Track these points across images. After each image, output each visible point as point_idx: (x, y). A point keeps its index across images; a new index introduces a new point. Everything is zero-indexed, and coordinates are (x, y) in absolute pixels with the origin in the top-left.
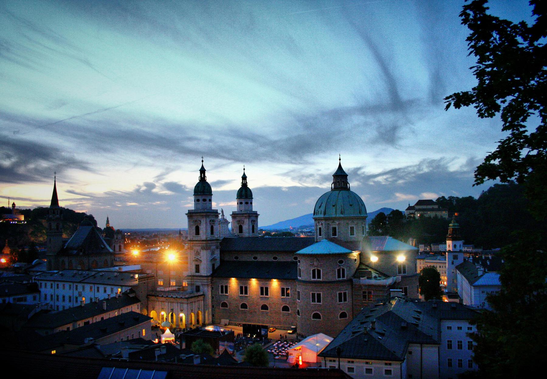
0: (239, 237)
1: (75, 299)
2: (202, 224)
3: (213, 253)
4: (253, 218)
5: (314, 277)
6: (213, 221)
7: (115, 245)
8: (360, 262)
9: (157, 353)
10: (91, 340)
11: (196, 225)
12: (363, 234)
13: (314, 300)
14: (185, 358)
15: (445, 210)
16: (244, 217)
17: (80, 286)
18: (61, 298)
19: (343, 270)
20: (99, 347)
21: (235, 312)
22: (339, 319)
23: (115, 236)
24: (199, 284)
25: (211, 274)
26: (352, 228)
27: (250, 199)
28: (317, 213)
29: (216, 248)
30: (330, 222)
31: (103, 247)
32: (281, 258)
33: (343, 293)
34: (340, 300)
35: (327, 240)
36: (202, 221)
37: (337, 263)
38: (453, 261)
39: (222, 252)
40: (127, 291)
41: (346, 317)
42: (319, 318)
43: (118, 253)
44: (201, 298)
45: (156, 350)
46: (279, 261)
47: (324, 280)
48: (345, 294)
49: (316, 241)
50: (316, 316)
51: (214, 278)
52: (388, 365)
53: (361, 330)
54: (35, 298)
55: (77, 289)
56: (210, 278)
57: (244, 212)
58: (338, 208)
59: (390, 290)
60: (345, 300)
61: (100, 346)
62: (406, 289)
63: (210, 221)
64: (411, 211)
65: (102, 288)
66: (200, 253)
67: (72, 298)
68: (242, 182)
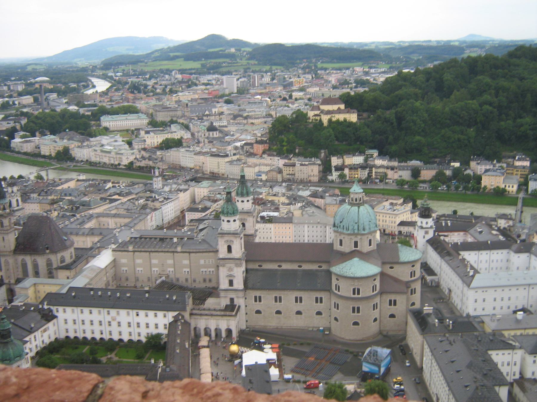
1: (107, 324)
5: (354, 294)
7: (11, 200)
13: (354, 311)
15: (354, 112)
17: (113, 312)
18: (87, 323)
19: (376, 285)
24: (232, 296)
26: (370, 241)
30: (353, 237)
31: (66, 239)
34: (374, 309)
36: (235, 242)
39: (247, 261)
48: (377, 303)
50: (356, 324)
54: (54, 325)
55: (109, 314)
58: (360, 225)
60: (377, 308)
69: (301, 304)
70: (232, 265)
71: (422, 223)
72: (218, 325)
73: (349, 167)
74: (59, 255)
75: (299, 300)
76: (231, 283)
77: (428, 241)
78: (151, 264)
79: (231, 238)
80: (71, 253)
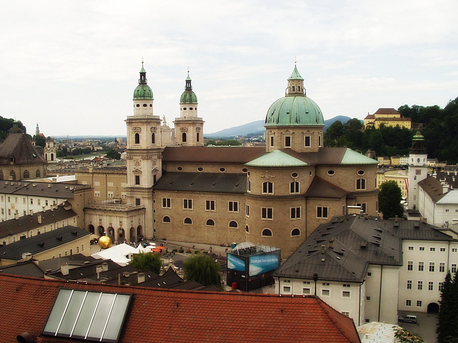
0: (182, 146)
2: (142, 131)
3: (154, 164)
4: (198, 126)
5: (265, 191)
6: (155, 128)
8: (315, 176)
9: (99, 270)
10: (29, 255)
11: (136, 133)
12: (320, 145)
13: (264, 216)
14: (128, 276)
15: (408, 120)
16: (188, 125)
17: (13, 198)
19: (297, 184)
20: (37, 262)
21: (178, 227)
22: (292, 236)
23: (47, 144)
24: (139, 196)
25: (152, 186)
26: (307, 139)
27: (194, 104)
28: (269, 120)
29: (158, 158)
31: (35, 156)
32: (230, 170)
33: (296, 209)
34: (293, 217)
35: (280, 151)
37: (291, 176)
38: (416, 176)
40: (62, 203)
41: (299, 234)
42: (271, 235)
43: (49, 162)
44: (142, 211)
45: (98, 267)
46: (226, 173)
47: (276, 195)
49: (267, 151)
51: (156, 191)
52: (347, 286)
53: (317, 249)
56: (151, 190)
57: (189, 119)
58: (292, 115)
59: (348, 206)
60: (298, 216)
61: (39, 262)
62: (364, 205)
63: (151, 129)
64: (371, 121)
65: (35, 200)
66: (140, 163)
67: (4, 210)
68: (186, 85)
69: (212, 211)
70: (139, 158)
71: (413, 159)
72: (111, 224)
73: (395, 166)
74: (23, 169)
75: (210, 205)
76: (138, 181)
77: (421, 184)
78: (106, 187)
79: (140, 125)
80: (38, 171)
